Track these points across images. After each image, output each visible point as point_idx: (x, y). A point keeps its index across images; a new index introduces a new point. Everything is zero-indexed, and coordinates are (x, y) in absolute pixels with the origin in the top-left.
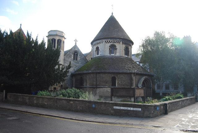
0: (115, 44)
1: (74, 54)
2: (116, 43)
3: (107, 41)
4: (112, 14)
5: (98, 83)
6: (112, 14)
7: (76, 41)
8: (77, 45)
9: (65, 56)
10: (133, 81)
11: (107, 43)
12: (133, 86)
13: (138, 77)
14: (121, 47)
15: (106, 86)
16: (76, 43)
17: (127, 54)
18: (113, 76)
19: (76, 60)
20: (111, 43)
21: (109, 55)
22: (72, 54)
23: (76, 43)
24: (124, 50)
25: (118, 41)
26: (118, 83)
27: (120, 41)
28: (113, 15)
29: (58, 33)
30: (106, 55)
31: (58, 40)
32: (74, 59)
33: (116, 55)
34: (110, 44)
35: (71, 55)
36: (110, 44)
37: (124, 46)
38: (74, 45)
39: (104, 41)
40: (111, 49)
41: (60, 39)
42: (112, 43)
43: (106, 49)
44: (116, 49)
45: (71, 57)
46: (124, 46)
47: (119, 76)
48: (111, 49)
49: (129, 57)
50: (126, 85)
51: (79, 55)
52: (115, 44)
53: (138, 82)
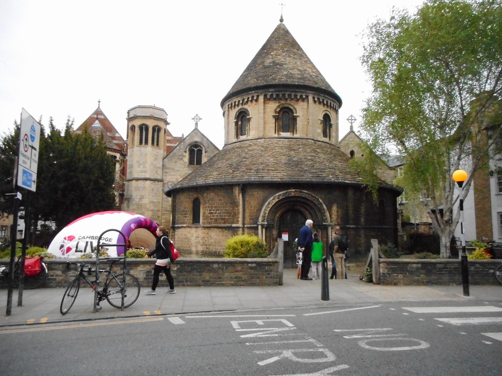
0: (246, 107)
1: (191, 152)
2: (249, 103)
3: (232, 104)
4: (281, 20)
5: (177, 216)
6: (281, 20)
7: (197, 119)
8: (200, 128)
9: (166, 160)
10: (238, 206)
11: (231, 107)
12: (238, 221)
13: (258, 194)
14: (262, 111)
15: (185, 224)
16: (197, 124)
17: (291, 126)
18: (195, 196)
19: (199, 162)
20: (238, 105)
21: (235, 140)
22: (185, 152)
23: (197, 124)
24: (274, 116)
25: (253, 97)
26: (204, 213)
27: (258, 96)
28: (283, 23)
29: (139, 113)
30: (230, 142)
31: (141, 127)
32: (191, 162)
33: (249, 138)
34: (237, 109)
35: (182, 156)
36: (237, 109)
37: (273, 106)
38: (194, 128)
39: (227, 105)
40: (240, 123)
41: (144, 124)
42: (240, 107)
43: (230, 127)
44: (249, 120)
45: (181, 159)
46: (273, 106)
47: (205, 195)
48: (240, 123)
49: (295, 136)
50: (222, 219)
51: (203, 152)
52: (246, 107)
53: (260, 210)
